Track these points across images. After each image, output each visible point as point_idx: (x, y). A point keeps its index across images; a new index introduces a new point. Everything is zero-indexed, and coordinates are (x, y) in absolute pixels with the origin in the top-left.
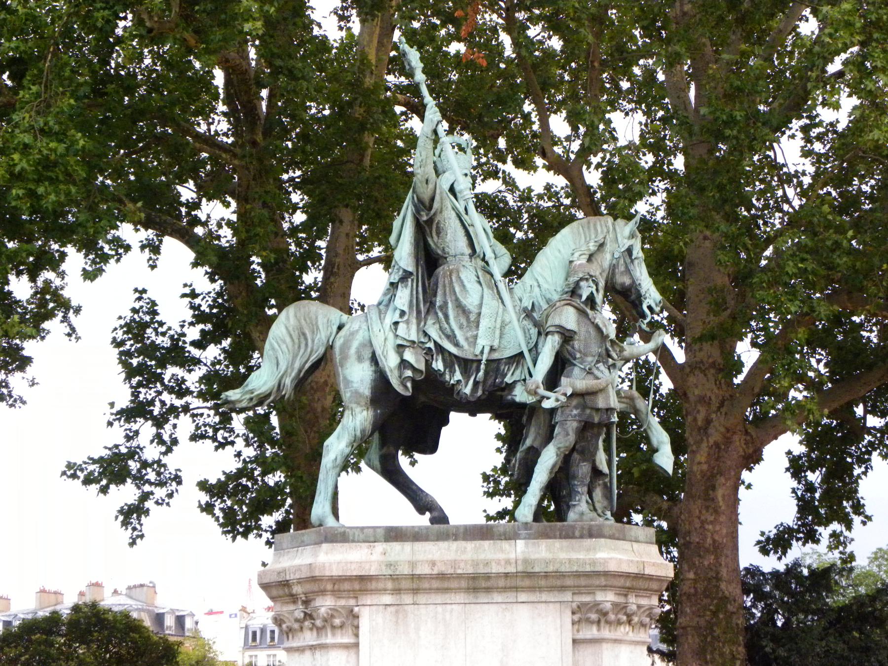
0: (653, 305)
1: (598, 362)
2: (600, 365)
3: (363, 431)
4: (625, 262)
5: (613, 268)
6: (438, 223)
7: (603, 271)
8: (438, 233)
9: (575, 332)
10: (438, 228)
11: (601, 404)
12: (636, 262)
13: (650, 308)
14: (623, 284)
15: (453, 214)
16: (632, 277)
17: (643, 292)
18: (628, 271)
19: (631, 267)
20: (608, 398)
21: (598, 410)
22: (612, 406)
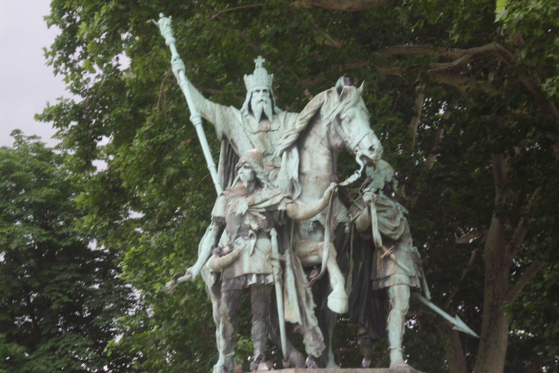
0: (367, 153)
1: (237, 237)
2: (240, 240)
3: (216, 318)
4: (334, 126)
5: (328, 133)
6: (232, 140)
7: (323, 140)
8: (236, 147)
9: (224, 219)
10: (234, 144)
11: (237, 273)
12: (343, 123)
13: (363, 157)
14: (337, 145)
15: (241, 129)
16: (341, 138)
17: (352, 146)
18: (337, 134)
19: (339, 129)
20: (241, 267)
21: (239, 278)
22: (246, 270)
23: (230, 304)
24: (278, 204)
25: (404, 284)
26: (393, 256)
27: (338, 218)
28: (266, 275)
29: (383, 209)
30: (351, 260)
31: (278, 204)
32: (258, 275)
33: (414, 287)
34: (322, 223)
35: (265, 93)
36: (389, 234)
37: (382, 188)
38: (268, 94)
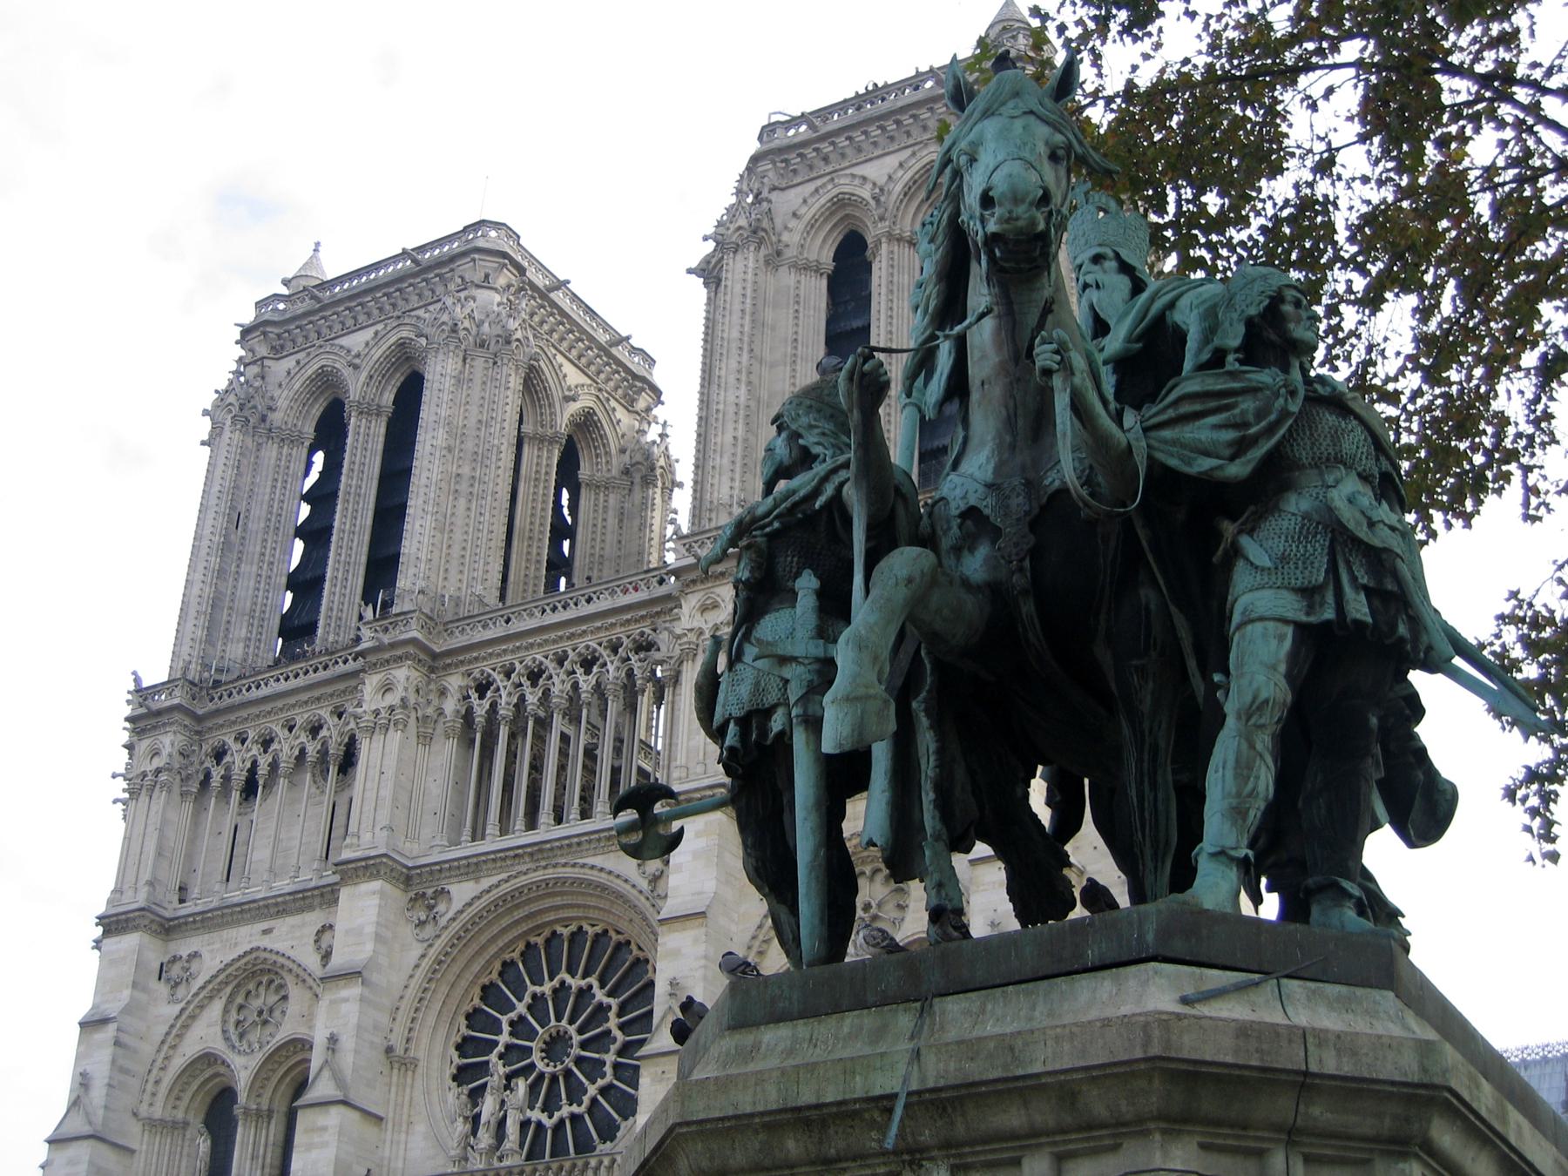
23: (749, 843)
24: (816, 492)
25: (1261, 619)
26: (1245, 541)
27: (1046, 482)
28: (767, 713)
29: (1213, 404)
30: (1173, 609)
31: (816, 492)
32: (744, 722)
33: (1328, 623)
34: (987, 512)
35: (1096, 268)
36: (1212, 469)
37: (1235, 342)
38: (1111, 265)
